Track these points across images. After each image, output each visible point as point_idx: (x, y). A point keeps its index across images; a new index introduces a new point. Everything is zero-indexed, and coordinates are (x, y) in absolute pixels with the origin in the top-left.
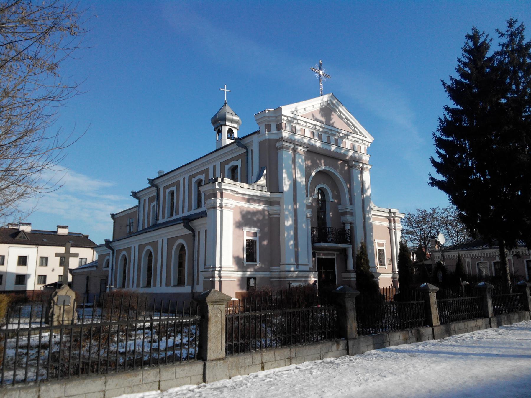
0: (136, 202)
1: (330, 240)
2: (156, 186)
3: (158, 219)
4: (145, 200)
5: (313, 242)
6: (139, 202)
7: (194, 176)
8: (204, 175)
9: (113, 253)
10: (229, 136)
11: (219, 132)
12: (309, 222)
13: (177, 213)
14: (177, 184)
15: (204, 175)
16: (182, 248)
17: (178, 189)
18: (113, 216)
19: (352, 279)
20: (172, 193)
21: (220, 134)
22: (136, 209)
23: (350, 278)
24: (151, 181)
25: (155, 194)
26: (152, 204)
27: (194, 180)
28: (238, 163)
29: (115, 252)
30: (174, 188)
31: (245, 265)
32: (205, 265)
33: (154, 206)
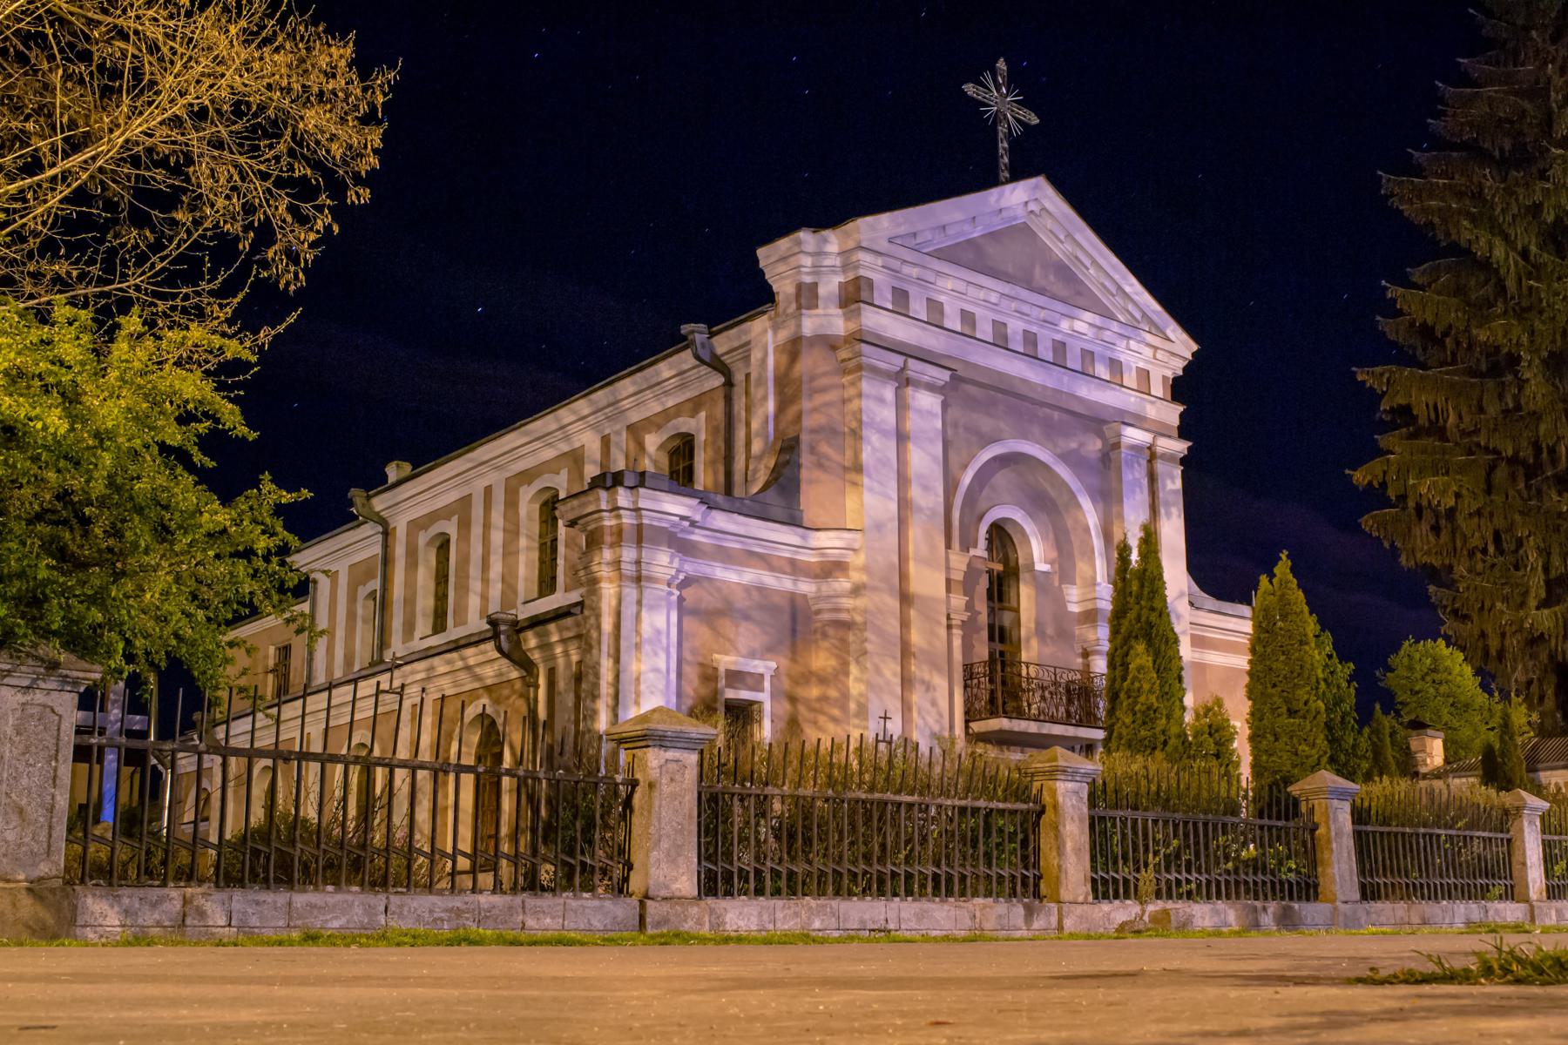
1: (1034, 711)
3: (383, 644)
13: (461, 621)
17: (465, 525)
20: (443, 545)
25: (377, 550)
26: (363, 591)
28: (698, 425)
33: (372, 595)
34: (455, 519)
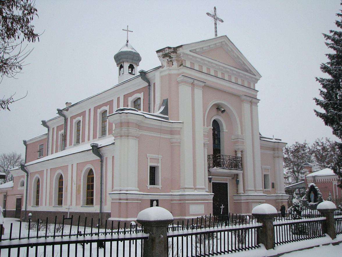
0: (45, 130)
2: (64, 116)
4: (53, 129)
5: (209, 167)
6: (48, 130)
7: (100, 107)
8: (108, 106)
9: (27, 175)
10: (130, 71)
11: (121, 67)
12: (206, 150)
14: (83, 114)
15: (108, 106)
16: (91, 172)
18: (25, 142)
19: (242, 201)
21: (122, 69)
22: (46, 137)
23: (241, 200)
24: (60, 112)
25: (63, 123)
27: (99, 111)
28: (141, 95)
29: (29, 174)
30: (80, 118)
31: (149, 188)
32: (113, 188)
34: (82, 116)
